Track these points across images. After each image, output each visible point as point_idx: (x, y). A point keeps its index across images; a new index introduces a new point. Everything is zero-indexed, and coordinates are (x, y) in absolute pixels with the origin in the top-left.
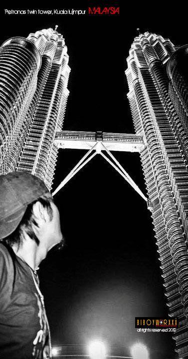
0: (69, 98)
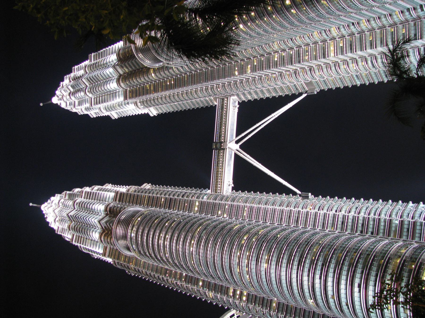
0: (153, 183)
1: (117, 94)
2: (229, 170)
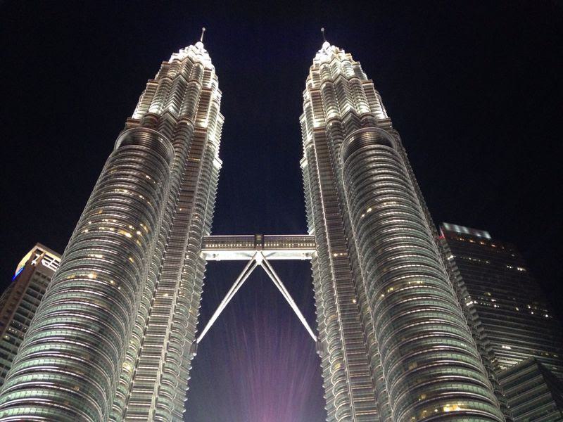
0: (222, 171)
1: (323, 119)
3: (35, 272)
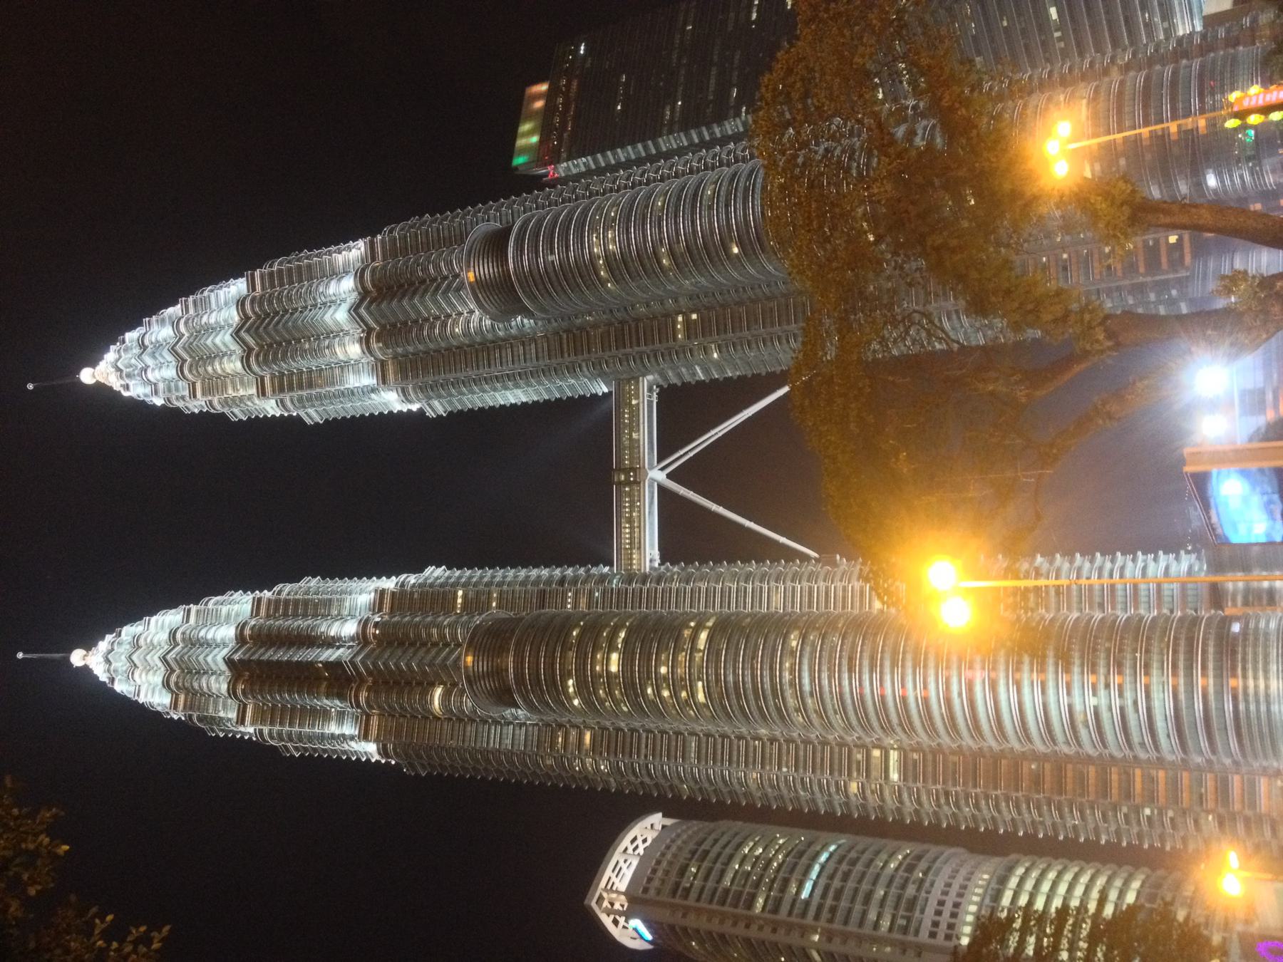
2: (652, 524)
3: (645, 896)
